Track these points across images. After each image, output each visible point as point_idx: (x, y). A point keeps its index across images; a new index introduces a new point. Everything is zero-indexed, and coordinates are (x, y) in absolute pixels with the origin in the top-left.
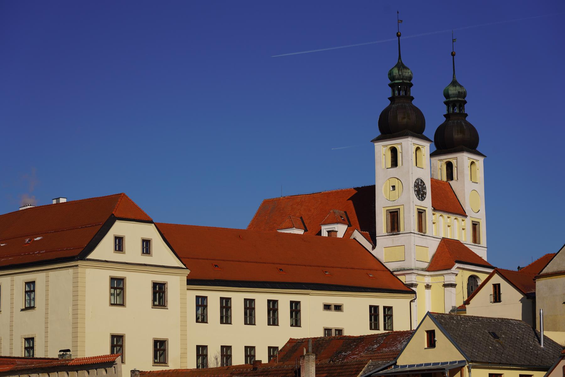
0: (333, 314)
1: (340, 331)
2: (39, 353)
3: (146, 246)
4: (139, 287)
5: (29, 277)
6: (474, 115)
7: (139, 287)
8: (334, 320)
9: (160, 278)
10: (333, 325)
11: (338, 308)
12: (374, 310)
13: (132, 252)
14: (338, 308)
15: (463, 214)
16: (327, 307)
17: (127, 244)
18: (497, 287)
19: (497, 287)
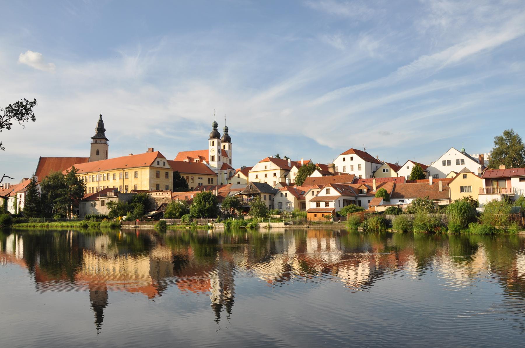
0: (200, 180)
1: (202, 184)
2: (139, 189)
3: (164, 163)
4: (162, 173)
5: (136, 171)
6: (230, 133)
7: (162, 173)
8: (200, 181)
9: (167, 171)
10: (201, 182)
11: (202, 178)
12: (209, 179)
13: (161, 165)
14: (202, 178)
15: (228, 157)
16: (199, 178)
17: (160, 163)
18: (238, 174)
19: (238, 174)
